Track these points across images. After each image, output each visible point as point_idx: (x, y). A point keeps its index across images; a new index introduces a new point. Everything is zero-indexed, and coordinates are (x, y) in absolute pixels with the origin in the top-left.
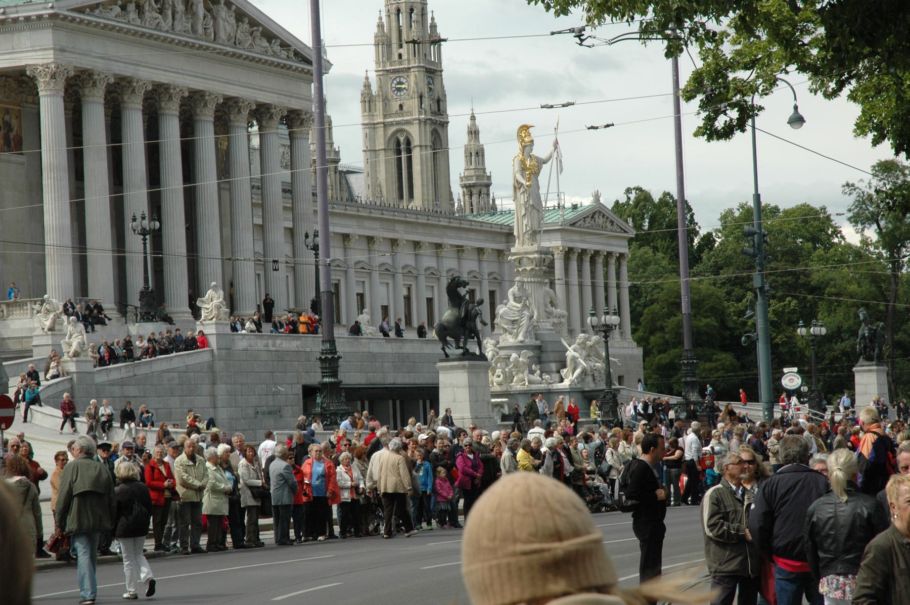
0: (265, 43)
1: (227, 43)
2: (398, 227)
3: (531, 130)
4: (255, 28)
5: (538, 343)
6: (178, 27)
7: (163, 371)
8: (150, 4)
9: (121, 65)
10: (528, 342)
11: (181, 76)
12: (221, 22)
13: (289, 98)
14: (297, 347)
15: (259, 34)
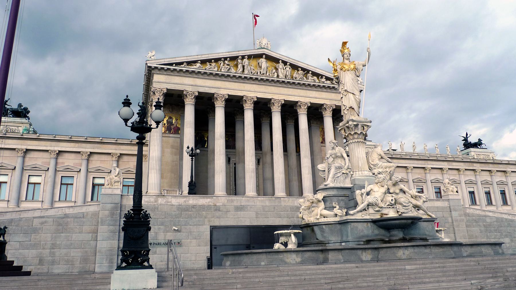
0: (315, 78)
1: (284, 78)
2: (475, 164)
3: (348, 45)
4: (306, 72)
5: (350, 185)
6: (246, 72)
7: (34, 218)
8: (224, 63)
9: (206, 88)
10: (332, 185)
11: (254, 93)
12: (279, 70)
13: (338, 102)
14: (206, 203)
15: (310, 75)
